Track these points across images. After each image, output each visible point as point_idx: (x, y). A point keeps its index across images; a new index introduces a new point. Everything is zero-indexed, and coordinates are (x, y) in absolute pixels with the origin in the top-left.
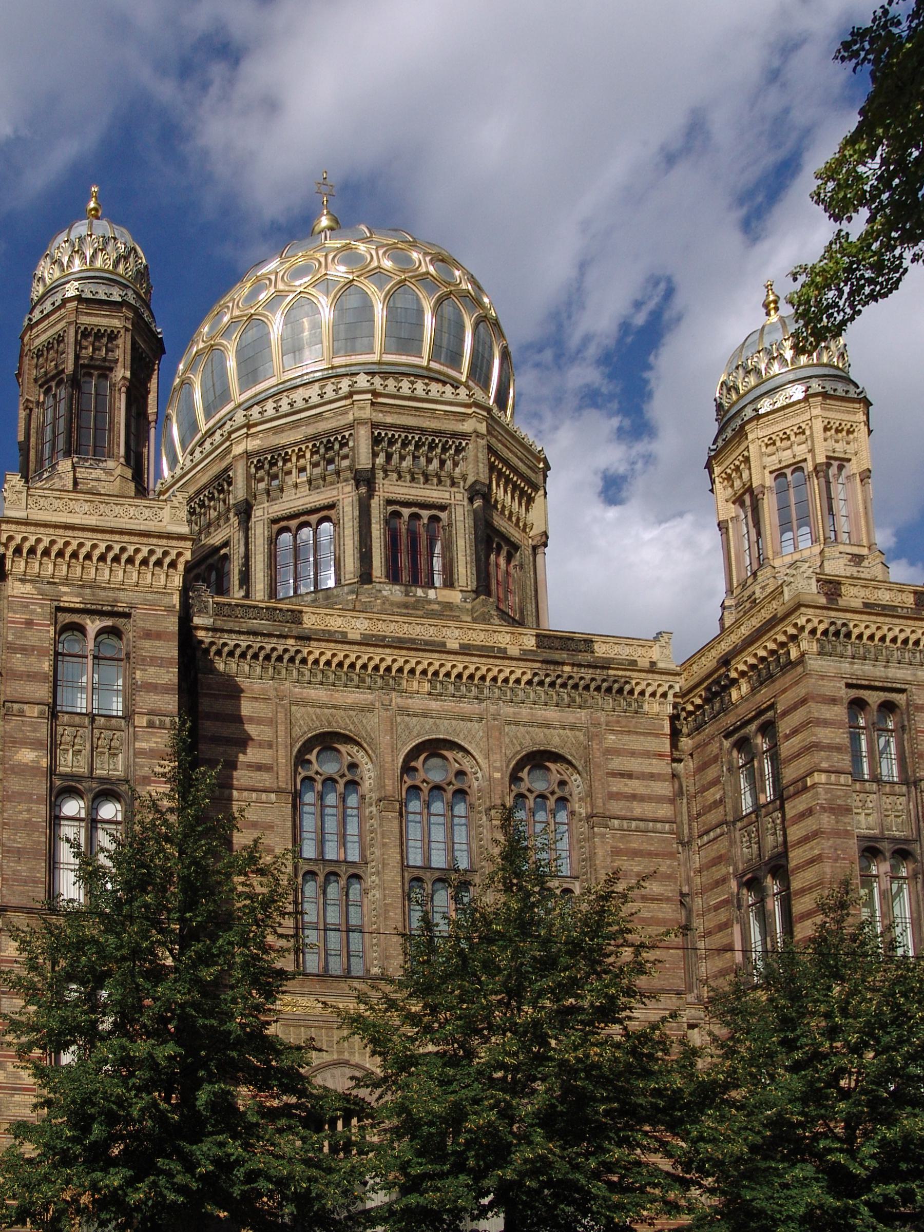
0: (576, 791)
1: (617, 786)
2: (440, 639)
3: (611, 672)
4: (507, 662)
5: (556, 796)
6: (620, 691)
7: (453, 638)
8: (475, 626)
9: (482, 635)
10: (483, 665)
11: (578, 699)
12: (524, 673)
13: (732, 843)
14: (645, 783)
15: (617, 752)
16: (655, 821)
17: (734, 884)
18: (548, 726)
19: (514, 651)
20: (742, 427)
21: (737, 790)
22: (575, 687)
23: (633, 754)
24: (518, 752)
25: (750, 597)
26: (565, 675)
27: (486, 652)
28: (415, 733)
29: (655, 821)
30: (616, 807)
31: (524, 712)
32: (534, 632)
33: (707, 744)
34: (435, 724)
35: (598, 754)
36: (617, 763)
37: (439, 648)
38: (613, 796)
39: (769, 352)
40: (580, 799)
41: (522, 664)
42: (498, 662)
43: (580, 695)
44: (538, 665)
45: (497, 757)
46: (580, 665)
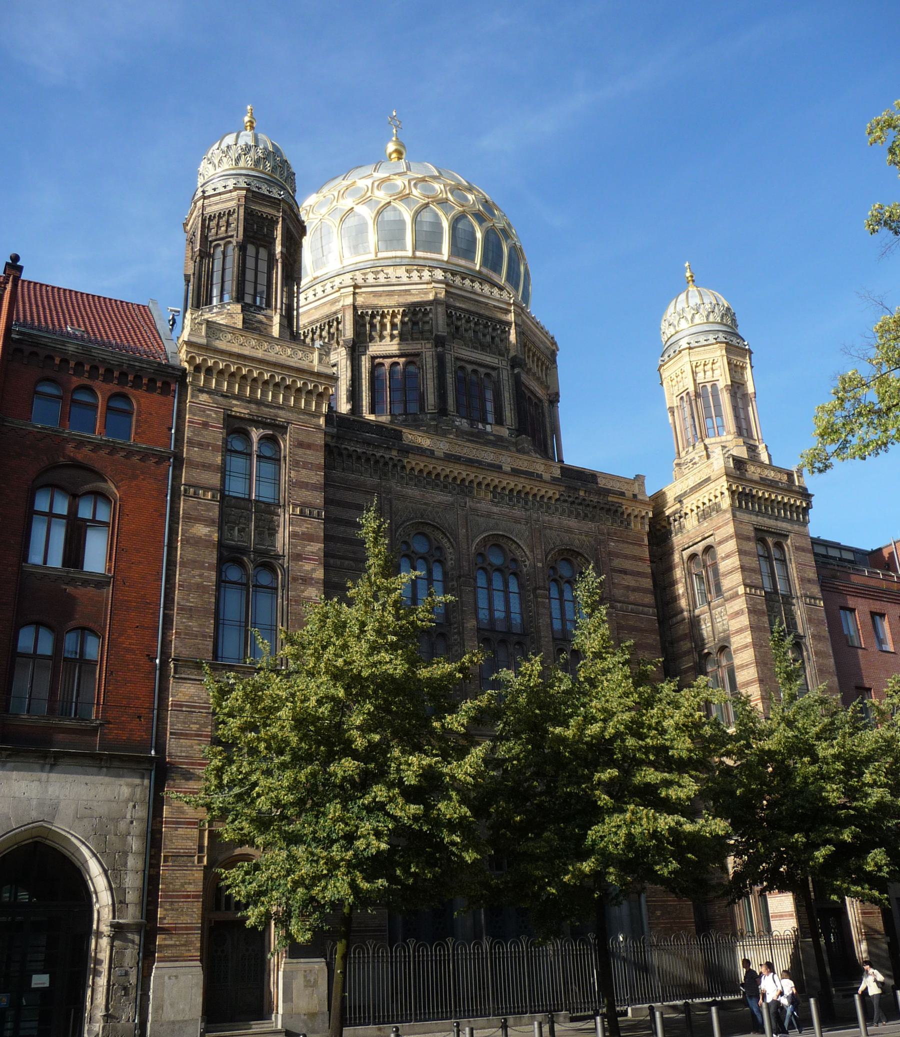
2: (497, 463)
4: (542, 484)
8: (521, 456)
9: (526, 463)
15: (617, 555)
18: (571, 532)
19: (546, 476)
23: (626, 557)
24: (552, 549)
25: (691, 460)
27: (529, 475)
34: (497, 524)
35: (604, 555)
37: (498, 468)
41: (552, 487)
42: (537, 484)
43: (591, 512)
45: (539, 551)
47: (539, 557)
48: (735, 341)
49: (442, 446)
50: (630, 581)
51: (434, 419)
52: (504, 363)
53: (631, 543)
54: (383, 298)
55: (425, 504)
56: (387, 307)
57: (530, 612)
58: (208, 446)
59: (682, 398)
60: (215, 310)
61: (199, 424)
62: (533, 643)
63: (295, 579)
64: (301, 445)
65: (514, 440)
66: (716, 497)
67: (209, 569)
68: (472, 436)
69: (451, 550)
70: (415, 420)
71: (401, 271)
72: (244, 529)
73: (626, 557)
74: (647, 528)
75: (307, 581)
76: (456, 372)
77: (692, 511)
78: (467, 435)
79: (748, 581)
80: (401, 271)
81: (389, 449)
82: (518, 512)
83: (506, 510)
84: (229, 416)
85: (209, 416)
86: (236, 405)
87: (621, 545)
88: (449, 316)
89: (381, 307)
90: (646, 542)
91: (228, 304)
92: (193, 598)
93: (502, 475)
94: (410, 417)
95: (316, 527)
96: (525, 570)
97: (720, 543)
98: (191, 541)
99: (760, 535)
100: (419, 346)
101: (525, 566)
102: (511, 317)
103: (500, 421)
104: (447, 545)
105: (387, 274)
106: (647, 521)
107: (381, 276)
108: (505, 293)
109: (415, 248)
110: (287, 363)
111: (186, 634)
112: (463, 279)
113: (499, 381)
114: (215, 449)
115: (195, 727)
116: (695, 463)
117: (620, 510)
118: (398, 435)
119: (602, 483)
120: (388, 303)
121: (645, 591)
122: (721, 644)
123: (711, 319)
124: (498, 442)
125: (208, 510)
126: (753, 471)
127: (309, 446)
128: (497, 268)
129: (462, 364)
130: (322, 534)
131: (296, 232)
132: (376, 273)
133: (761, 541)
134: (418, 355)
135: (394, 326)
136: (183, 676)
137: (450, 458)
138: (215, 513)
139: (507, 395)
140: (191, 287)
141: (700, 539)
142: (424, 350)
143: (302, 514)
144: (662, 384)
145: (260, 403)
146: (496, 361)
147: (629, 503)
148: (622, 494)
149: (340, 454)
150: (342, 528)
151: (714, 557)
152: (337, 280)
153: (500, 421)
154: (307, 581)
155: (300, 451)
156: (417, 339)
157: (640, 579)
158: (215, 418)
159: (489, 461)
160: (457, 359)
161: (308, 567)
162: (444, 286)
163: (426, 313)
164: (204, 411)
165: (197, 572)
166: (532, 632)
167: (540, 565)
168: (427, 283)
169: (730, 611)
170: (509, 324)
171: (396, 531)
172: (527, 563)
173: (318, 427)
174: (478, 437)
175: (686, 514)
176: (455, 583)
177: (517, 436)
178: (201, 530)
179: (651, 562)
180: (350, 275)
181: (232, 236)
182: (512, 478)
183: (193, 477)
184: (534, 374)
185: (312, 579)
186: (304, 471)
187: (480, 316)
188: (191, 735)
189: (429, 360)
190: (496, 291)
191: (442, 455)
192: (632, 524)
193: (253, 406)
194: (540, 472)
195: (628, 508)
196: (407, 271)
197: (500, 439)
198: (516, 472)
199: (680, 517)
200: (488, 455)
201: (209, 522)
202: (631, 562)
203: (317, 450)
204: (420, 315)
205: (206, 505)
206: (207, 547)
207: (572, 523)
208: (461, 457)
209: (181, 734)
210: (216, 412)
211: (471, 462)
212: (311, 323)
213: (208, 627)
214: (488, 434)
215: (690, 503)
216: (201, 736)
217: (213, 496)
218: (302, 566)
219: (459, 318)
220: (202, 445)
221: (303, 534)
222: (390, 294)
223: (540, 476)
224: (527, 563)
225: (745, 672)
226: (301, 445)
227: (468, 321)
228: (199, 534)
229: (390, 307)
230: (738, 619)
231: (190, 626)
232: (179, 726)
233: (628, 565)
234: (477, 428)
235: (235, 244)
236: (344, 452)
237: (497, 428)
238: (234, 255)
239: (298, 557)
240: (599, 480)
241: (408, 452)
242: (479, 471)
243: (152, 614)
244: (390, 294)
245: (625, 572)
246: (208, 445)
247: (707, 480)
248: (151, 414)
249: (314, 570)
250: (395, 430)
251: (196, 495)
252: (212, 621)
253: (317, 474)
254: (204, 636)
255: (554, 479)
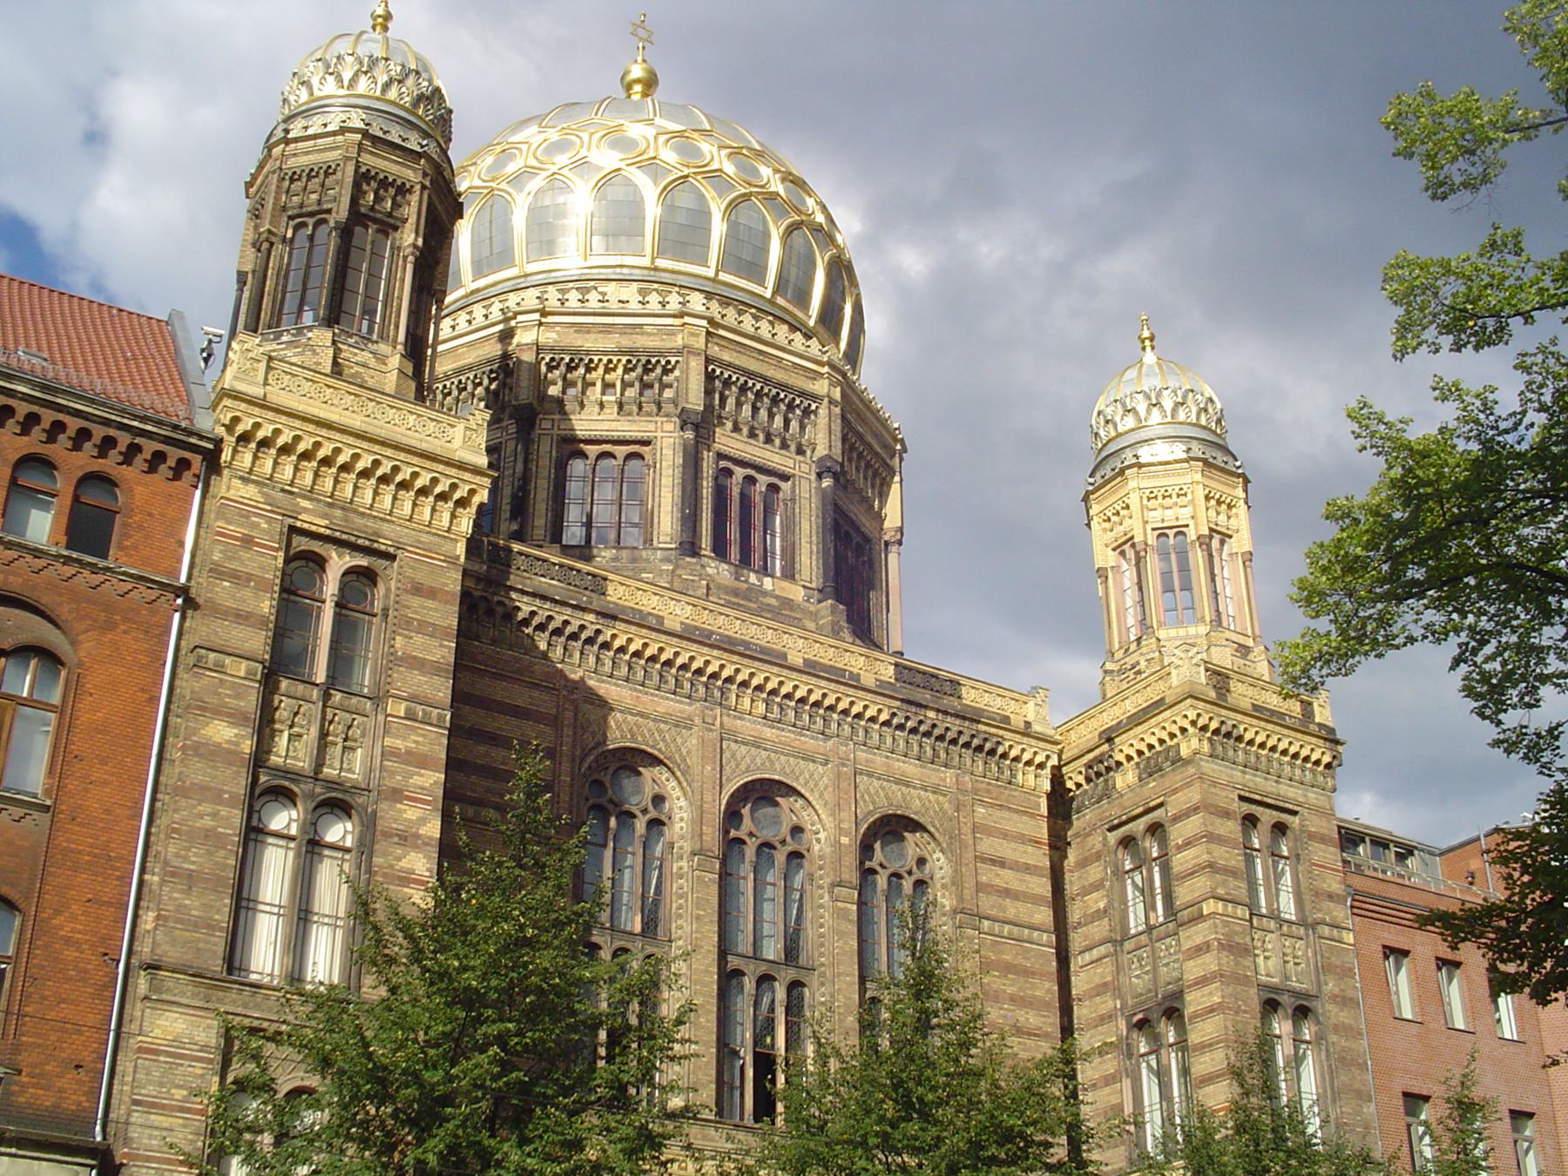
0: (938, 874)
1: (988, 875)
3: (982, 728)
4: (860, 694)
5: (914, 878)
6: (992, 752)
7: (797, 649)
10: (831, 693)
11: (943, 755)
12: (880, 711)
13: (1119, 969)
14: (1020, 875)
15: (989, 831)
16: (1032, 928)
17: (1122, 1024)
19: (868, 680)
20: (1122, 472)
21: (1125, 902)
22: (941, 738)
23: (1005, 835)
24: (870, 813)
26: (929, 722)
27: (838, 676)
28: (743, 767)
29: (1032, 928)
30: (987, 903)
31: (879, 761)
32: (893, 660)
33: (1089, 835)
36: (988, 845)
37: (776, 659)
38: (980, 887)
39: (1148, 397)
40: (944, 886)
41: (879, 699)
42: (851, 691)
44: (898, 703)
46: (946, 713)
47: (844, 826)
48: (1220, 458)
49: (678, 613)
50: (1006, 878)
51: (668, 560)
52: (805, 468)
53: (1017, 811)
54: (593, 336)
55: (641, 714)
56: (597, 353)
57: (822, 926)
58: (249, 580)
59: (1123, 553)
60: (285, 339)
61: (236, 539)
62: (823, 984)
63: (387, 835)
64: (418, 590)
65: (812, 608)
66: (1172, 736)
67: (230, 803)
68: (736, 595)
69: (682, 802)
70: (634, 560)
71: (630, 292)
72: (300, 736)
73: (1005, 835)
74: (1047, 786)
75: (408, 839)
76: (716, 479)
77: (1129, 758)
78: (726, 593)
79: (1220, 891)
80: (630, 292)
81: (584, 610)
82: (810, 743)
83: (788, 736)
84: (293, 530)
85: (256, 526)
86: (306, 510)
87: (998, 813)
88: (710, 377)
89: (588, 352)
90: (1044, 810)
91: (310, 328)
92: (195, 855)
93: (785, 672)
94: (624, 554)
95: (435, 742)
96: (817, 847)
97: (1176, 819)
98: (202, 750)
99: (1247, 808)
100: (651, 427)
101: (818, 841)
102: (821, 387)
103: (790, 574)
104: (677, 793)
105: (604, 294)
106: (1047, 771)
107: (593, 297)
108: (814, 343)
109: (660, 252)
110: (405, 440)
111: (178, 921)
112: (740, 312)
113: (793, 500)
114: (263, 585)
115: (179, 1094)
116: (1139, 672)
117: (1000, 750)
118: (598, 584)
119: (970, 696)
120: (600, 346)
121: (1036, 900)
122: (1167, 1004)
123: (1182, 416)
124: (783, 612)
125: (238, 696)
126: (1242, 694)
127: (431, 593)
128: (803, 299)
129: (729, 465)
130: (444, 756)
131: (444, 208)
132: (587, 290)
133: (1250, 821)
134: (646, 443)
135: (607, 386)
136: (164, 997)
137: (688, 635)
138: (250, 702)
139: (805, 525)
140: (246, 294)
141: (1141, 809)
142: (659, 434)
143: (410, 716)
144: (1088, 525)
145: (348, 507)
146: (790, 463)
147: (1018, 737)
148: (1006, 719)
149: (490, 612)
150: (483, 749)
151: (1163, 842)
152: (513, 299)
153: (790, 574)
154: (408, 839)
155: (415, 602)
156: (649, 414)
157: (1028, 877)
158: (267, 530)
159: (762, 643)
160: (720, 456)
161: (411, 813)
162: (704, 323)
163: (666, 371)
164: (247, 515)
165: (205, 808)
166: (822, 965)
167: (845, 840)
168: (674, 316)
169: (1186, 945)
170: (815, 397)
171: (582, 760)
172: (822, 835)
173: (451, 560)
174: (745, 600)
175: (1119, 764)
176: (684, 863)
177: (820, 601)
178: (222, 732)
179: (1051, 847)
180: (535, 292)
181: (329, 211)
182: (805, 678)
183: (216, 633)
184: (858, 491)
185: (417, 836)
186: (419, 639)
187: (766, 380)
188: (172, 1108)
189: (668, 452)
190: (798, 337)
191: (678, 628)
192: (1020, 775)
193: (338, 513)
194: (855, 671)
195: (1015, 746)
196: (640, 291)
197: (787, 603)
198: (811, 669)
199: (1108, 769)
200: (761, 634)
201: (236, 718)
202: (1013, 845)
203: (447, 602)
204: (659, 370)
205: (234, 686)
206: (230, 764)
207: (911, 768)
208: (712, 633)
209: (154, 1105)
210: (269, 520)
211: (728, 646)
212: (459, 371)
213: (218, 912)
214: (765, 594)
215: (1126, 746)
216: (189, 1111)
217: (249, 672)
218: (400, 811)
219: (727, 383)
220: (238, 578)
221: (409, 752)
222: (607, 329)
223: (857, 677)
224: (822, 835)
225: (1206, 1058)
226: (418, 590)
227: (743, 389)
228: (217, 739)
229: (605, 353)
230: (1199, 961)
231: (186, 906)
232: (151, 1089)
233: (1006, 850)
234: (746, 581)
235: (332, 224)
236: (500, 609)
237: (785, 584)
238: (328, 244)
239: (397, 795)
240: (964, 690)
241: (615, 618)
242: (745, 661)
243: (118, 878)
244: (607, 329)
245: (1001, 863)
246: (249, 577)
247: (1158, 706)
248: (150, 514)
249: (423, 821)
250: (594, 576)
251: (219, 668)
252: (228, 901)
253: (441, 645)
254: (212, 927)
255: (882, 683)
